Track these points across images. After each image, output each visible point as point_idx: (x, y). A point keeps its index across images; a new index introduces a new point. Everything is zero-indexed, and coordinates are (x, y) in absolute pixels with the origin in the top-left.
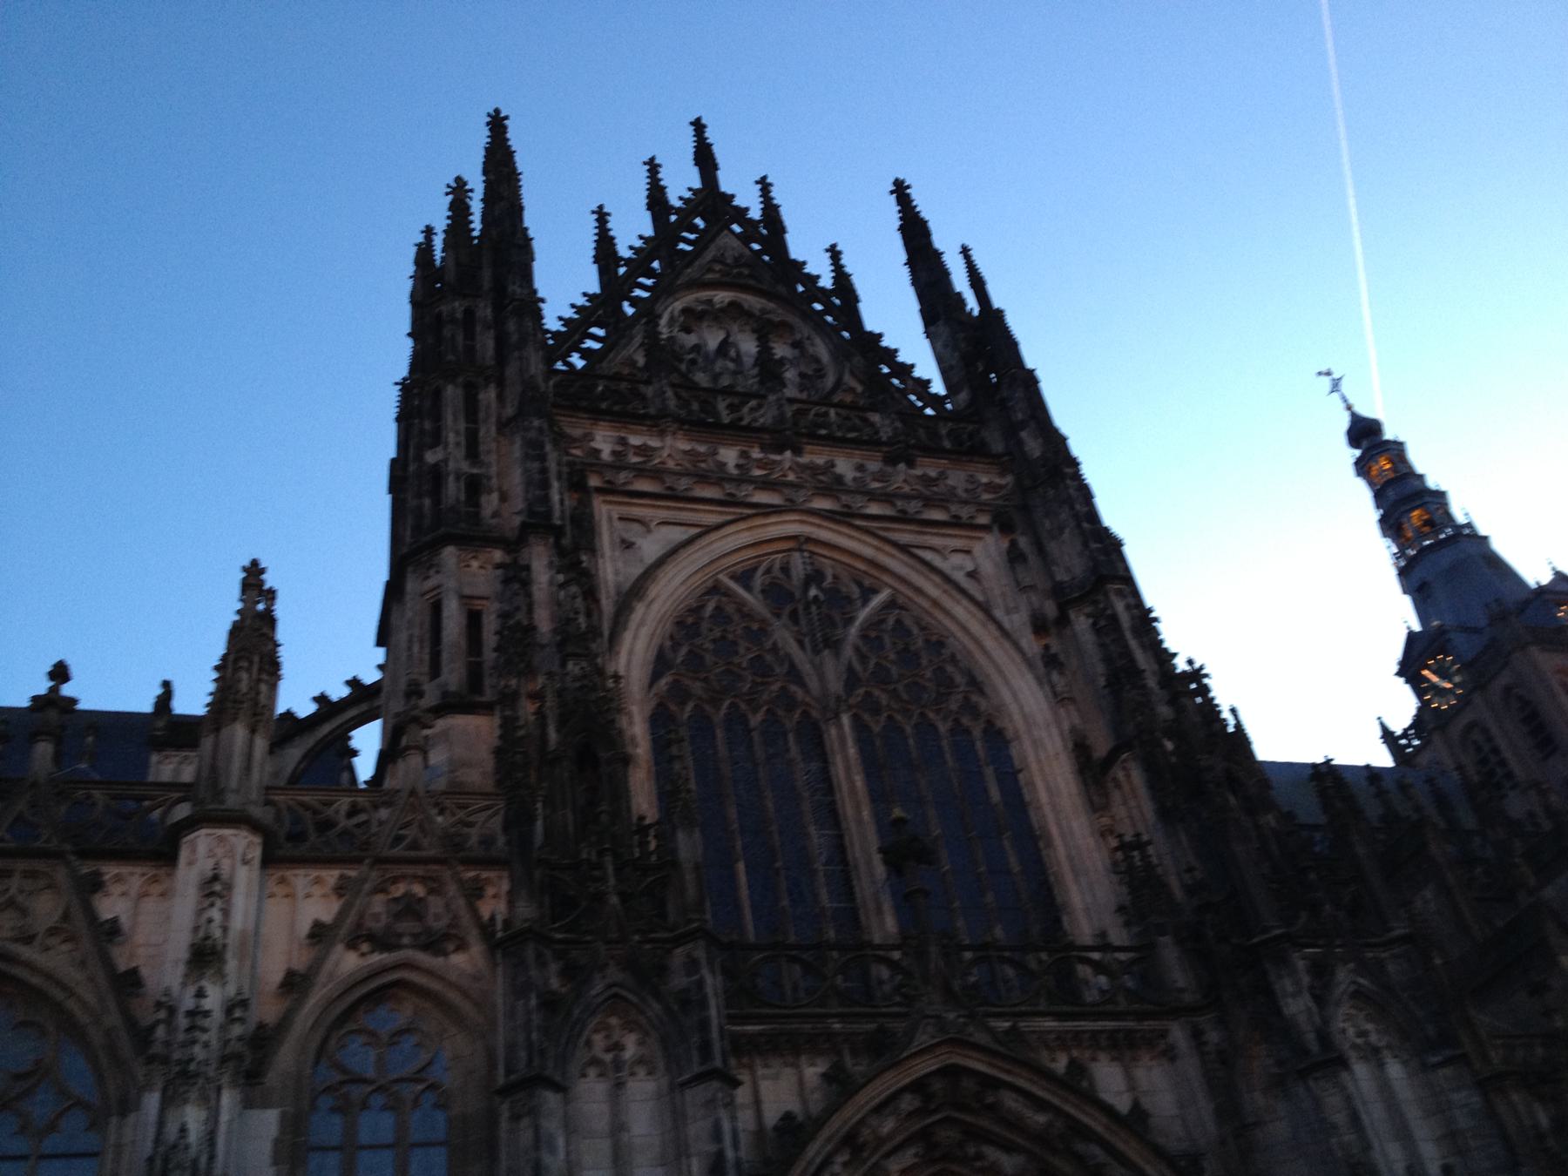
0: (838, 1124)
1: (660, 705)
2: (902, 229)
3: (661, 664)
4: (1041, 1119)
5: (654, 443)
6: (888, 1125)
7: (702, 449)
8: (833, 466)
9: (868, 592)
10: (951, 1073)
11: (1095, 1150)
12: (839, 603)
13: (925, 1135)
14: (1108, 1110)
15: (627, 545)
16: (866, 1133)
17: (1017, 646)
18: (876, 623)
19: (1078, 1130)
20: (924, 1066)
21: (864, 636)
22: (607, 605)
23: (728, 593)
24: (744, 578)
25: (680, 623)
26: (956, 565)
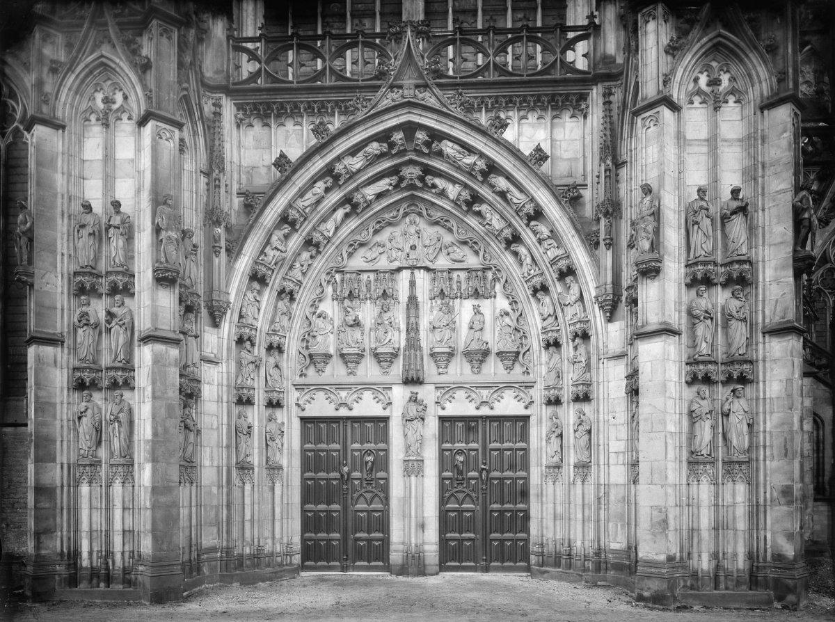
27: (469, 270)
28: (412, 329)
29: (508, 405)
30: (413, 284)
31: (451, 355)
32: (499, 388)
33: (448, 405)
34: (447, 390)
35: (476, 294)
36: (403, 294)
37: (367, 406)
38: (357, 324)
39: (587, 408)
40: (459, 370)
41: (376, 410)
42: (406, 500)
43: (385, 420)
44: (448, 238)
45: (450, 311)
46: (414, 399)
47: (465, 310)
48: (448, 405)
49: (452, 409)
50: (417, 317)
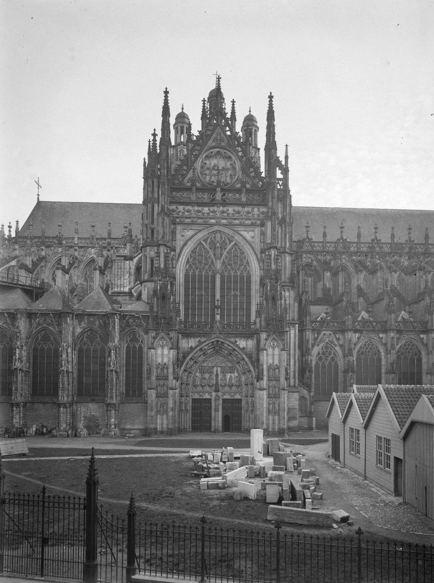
0: (199, 348)
1: (187, 270)
2: (268, 113)
3: (188, 262)
4: (229, 348)
5: (191, 208)
6: (206, 347)
7: (200, 209)
8: (228, 210)
9: (231, 241)
10: (217, 341)
11: (237, 353)
12: (223, 246)
13: (214, 347)
14: (239, 348)
15: (183, 236)
16: (203, 348)
17: (257, 256)
18: (230, 249)
19: (234, 349)
20: (214, 340)
21: (228, 253)
22: (178, 251)
23: (203, 245)
24: (205, 241)
25: (192, 252)
26: (248, 235)
27: (229, 367)
28: (217, 380)
29: (237, 396)
30: (217, 370)
31: (225, 386)
32: (235, 393)
33: (224, 396)
34: (224, 393)
35: (231, 373)
36: (215, 373)
37: (207, 396)
38: (205, 379)
39: (253, 399)
40: (227, 389)
41: (209, 397)
42: (215, 417)
43: (211, 399)
44: (225, 360)
45: (225, 376)
46: (217, 395)
47: (228, 376)
48: (224, 396)
49: (225, 397)
50: (218, 378)
